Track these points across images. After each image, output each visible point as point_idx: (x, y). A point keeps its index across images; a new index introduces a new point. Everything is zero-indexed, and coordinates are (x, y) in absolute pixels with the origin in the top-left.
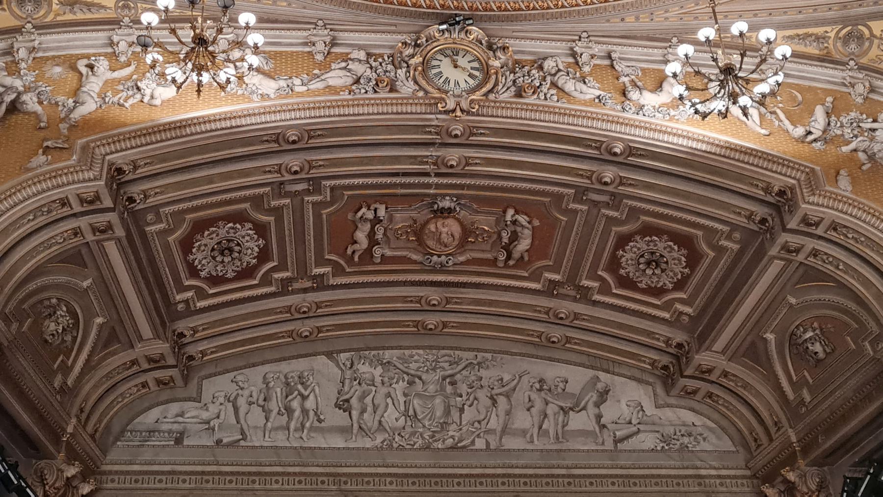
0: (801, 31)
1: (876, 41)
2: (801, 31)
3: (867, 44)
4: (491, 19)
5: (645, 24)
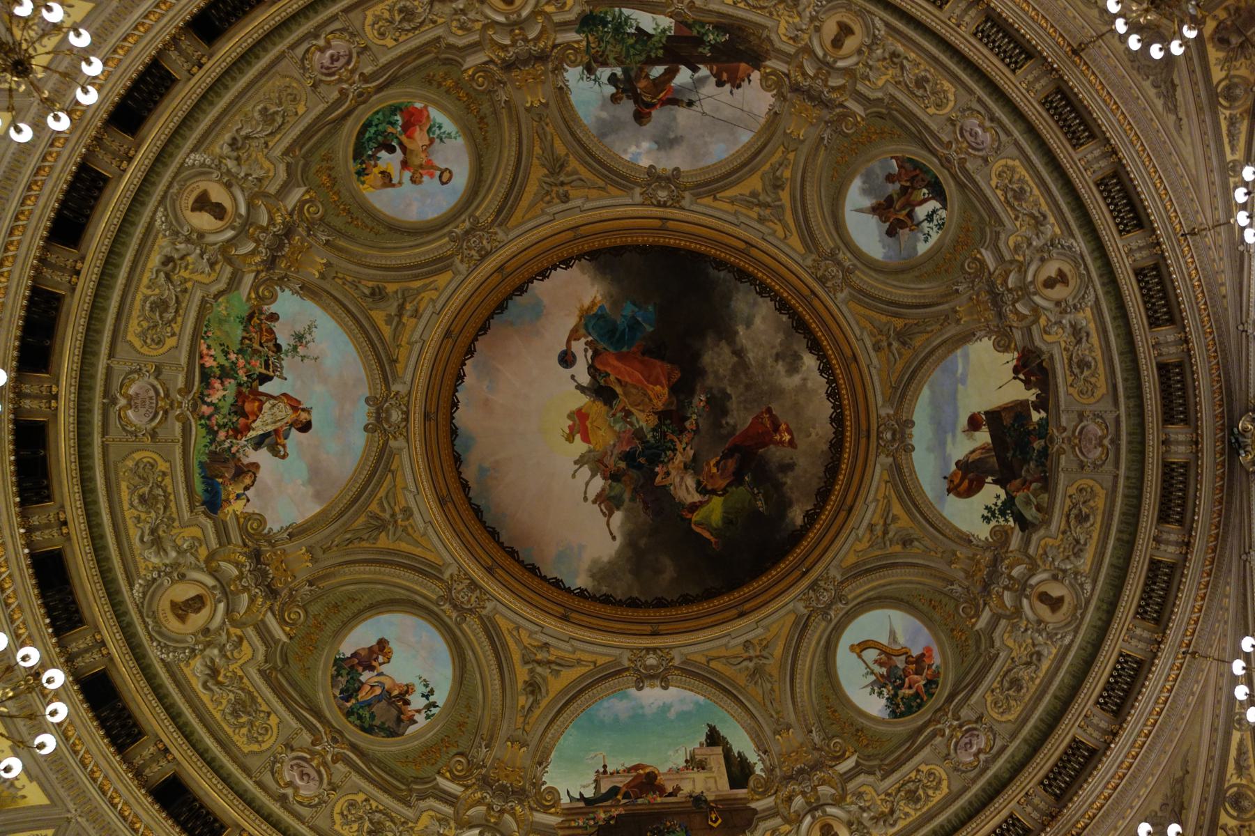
0: (1226, 140)
1: (1232, 73)
2: (1226, 140)
3: (1236, 80)
4: (1230, 411)
5: (1226, 278)
